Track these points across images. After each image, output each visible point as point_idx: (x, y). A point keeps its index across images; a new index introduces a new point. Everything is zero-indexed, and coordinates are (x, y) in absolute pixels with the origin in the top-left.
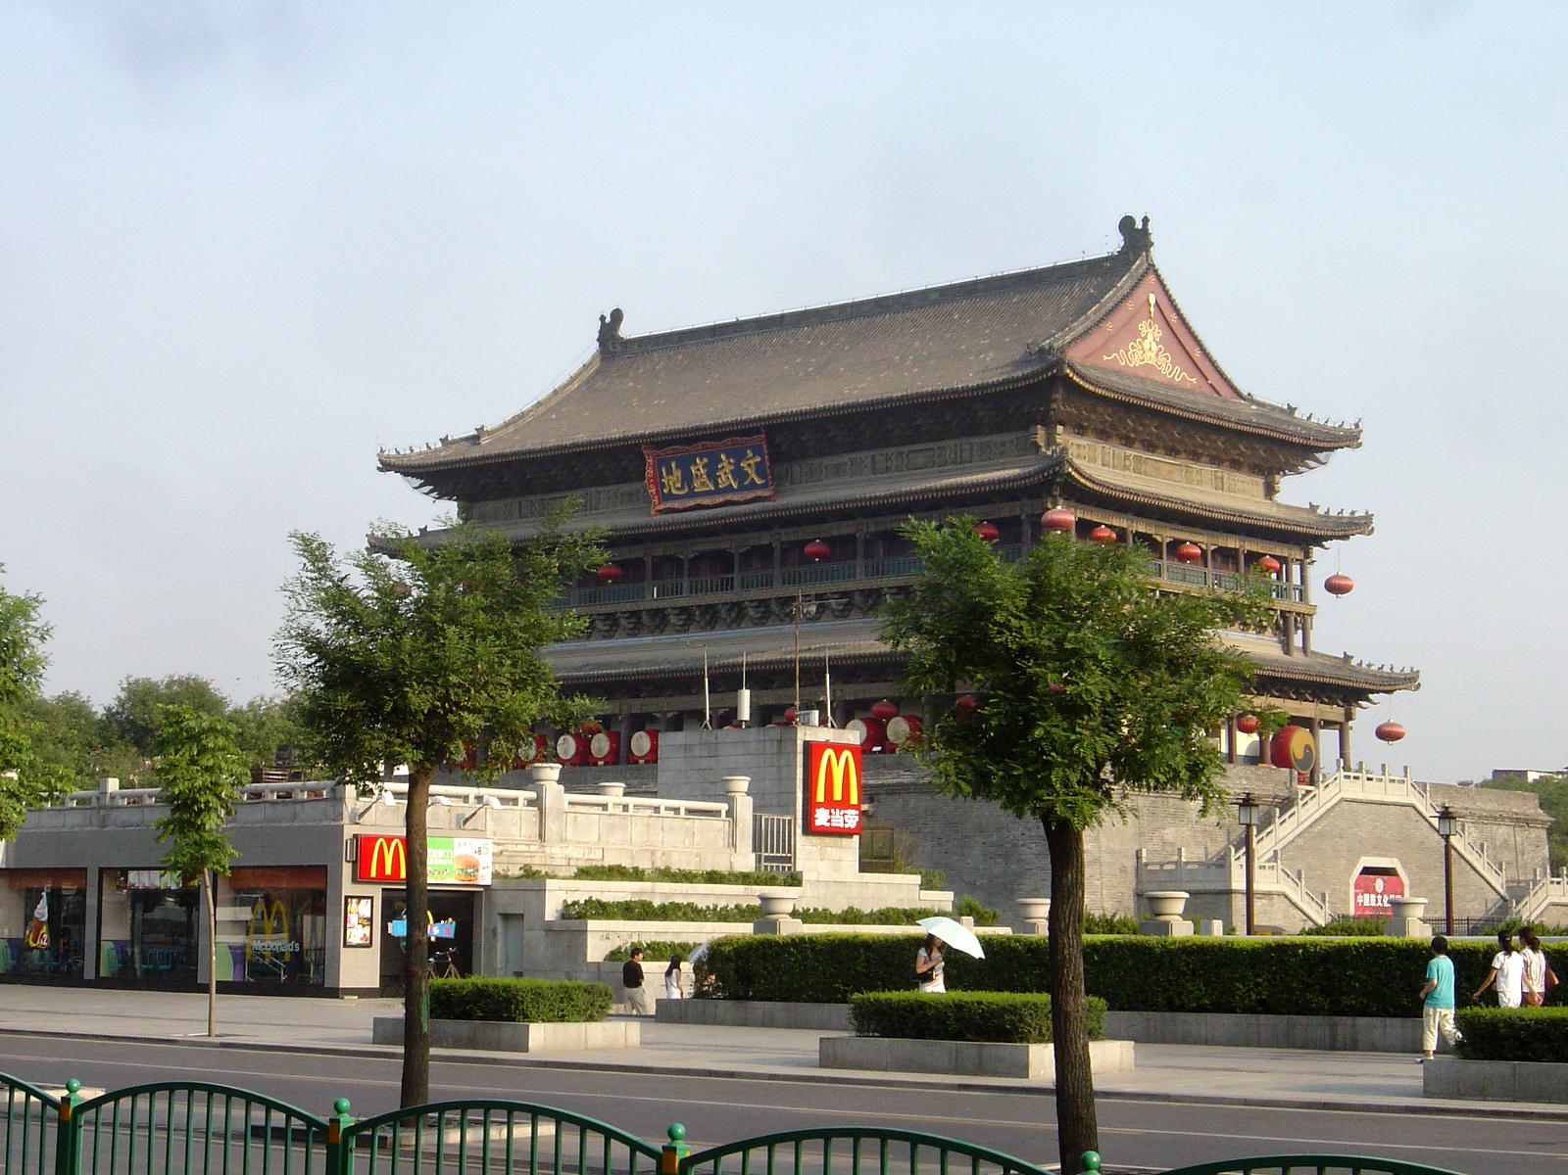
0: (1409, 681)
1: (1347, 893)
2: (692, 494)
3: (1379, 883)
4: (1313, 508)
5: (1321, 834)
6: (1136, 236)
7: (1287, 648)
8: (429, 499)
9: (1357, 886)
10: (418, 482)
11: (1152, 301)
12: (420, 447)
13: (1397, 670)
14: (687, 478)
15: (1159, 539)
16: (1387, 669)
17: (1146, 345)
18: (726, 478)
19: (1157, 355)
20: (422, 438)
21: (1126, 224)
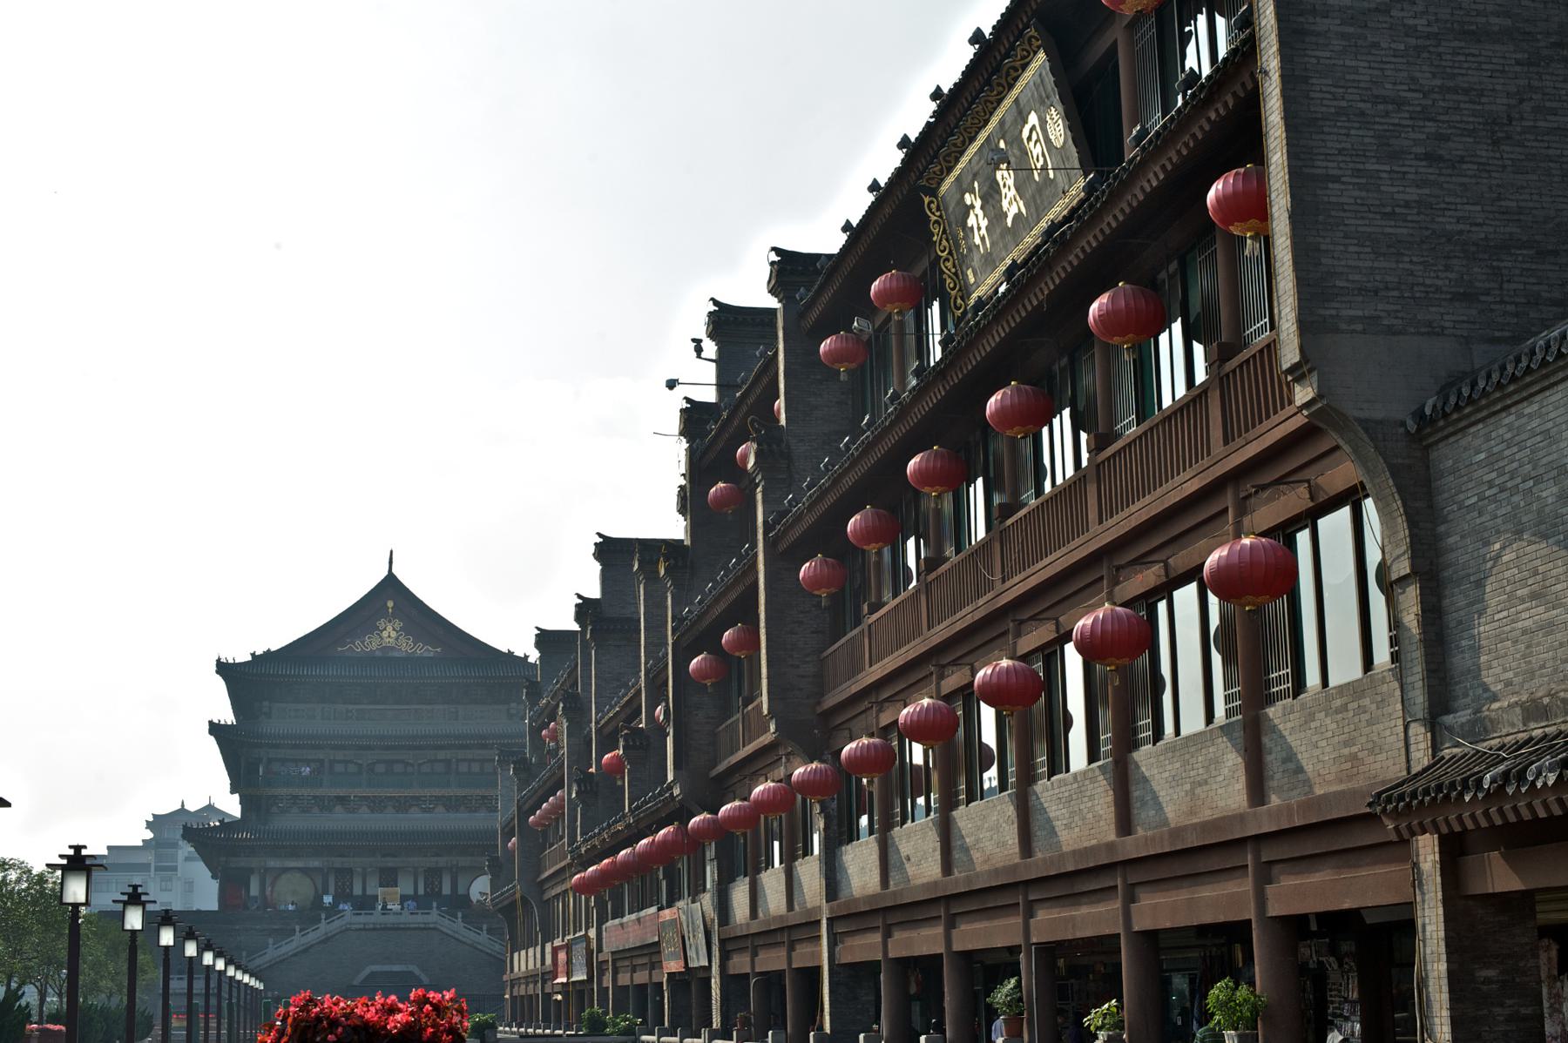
11: (390, 604)
17: (385, 634)
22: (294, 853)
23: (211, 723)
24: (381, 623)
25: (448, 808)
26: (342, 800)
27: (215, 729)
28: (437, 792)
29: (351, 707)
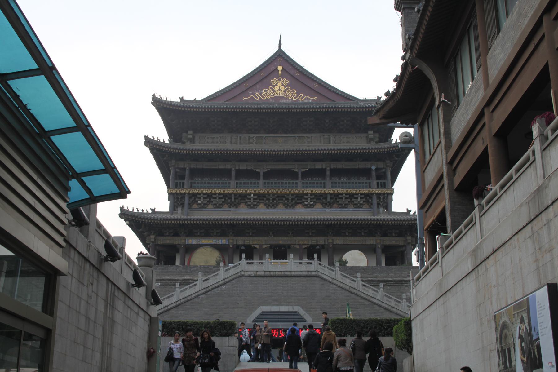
11: (280, 68)
17: (276, 88)
19: (285, 91)
22: (207, 234)
23: (146, 137)
24: (274, 81)
25: (325, 205)
26: (243, 197)
27: (151, 144)
28: (316, 191)
29: (252, 136)
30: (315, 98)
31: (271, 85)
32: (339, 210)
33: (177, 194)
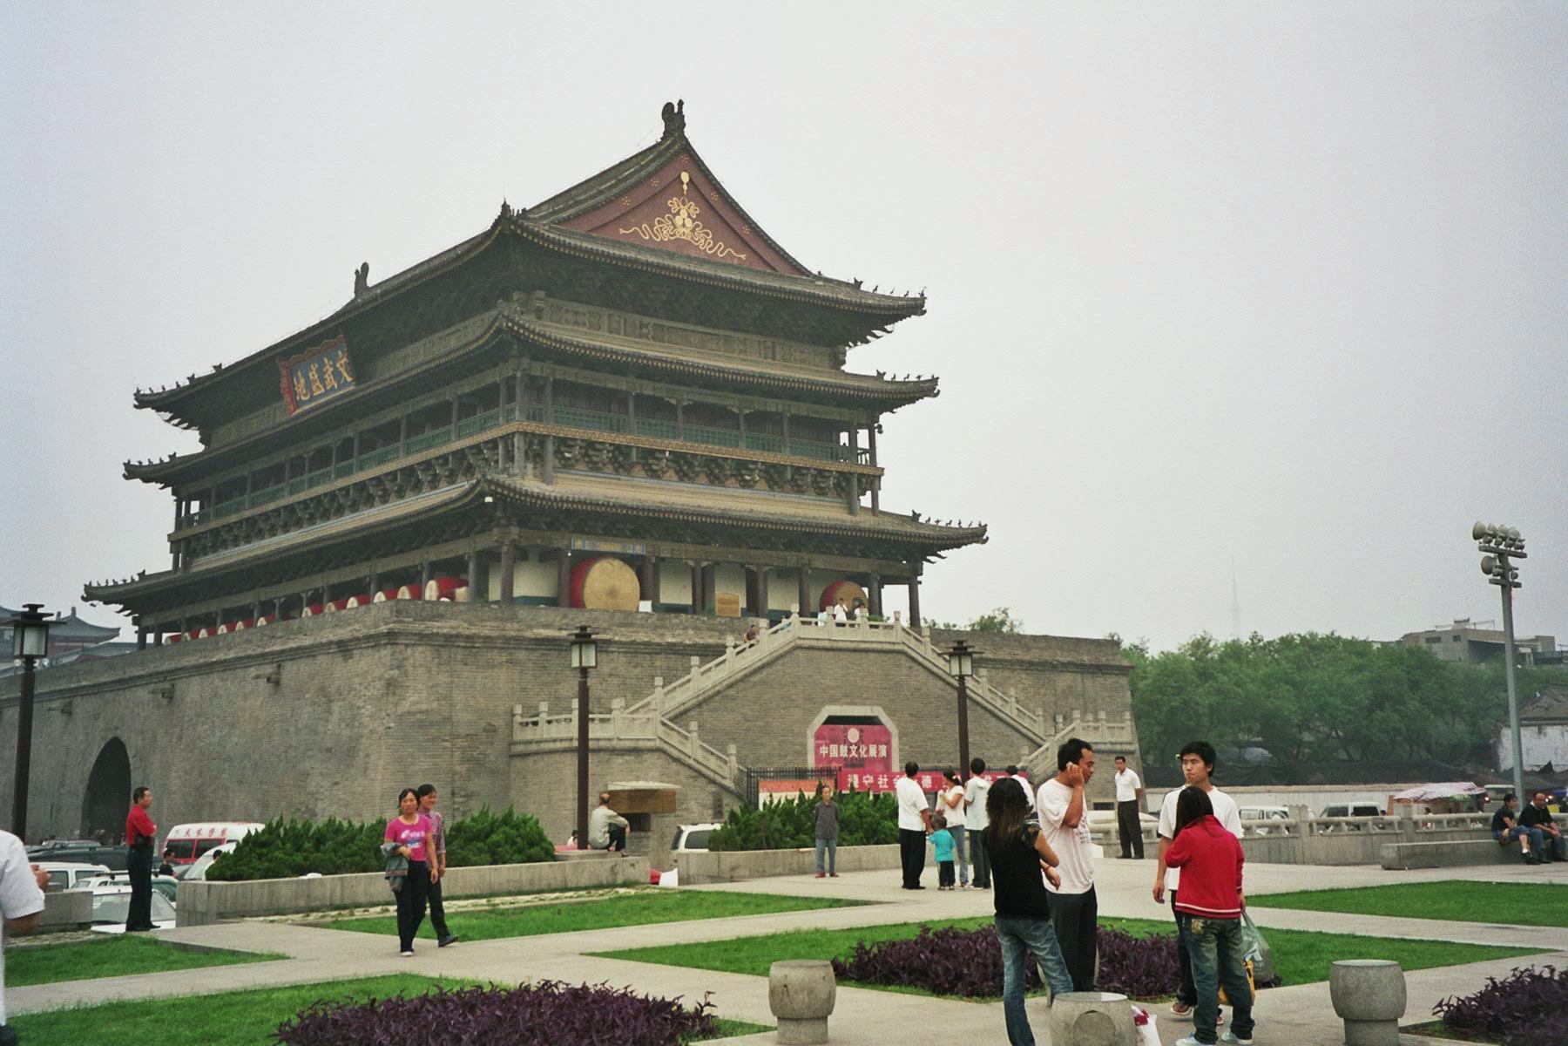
0: (977, 535)
1: (804, 745)
2: (313, 398)
3: (853, 734)
4: (881, 375)
5: (763, 682)
6: (673, 117)
7: (851, 508)
8: (178, 429)
9: (818, 736)
10: (168, 415)
11: (685, 177)
12: (171, 386)
13: (965, 525)
14: (308, 385)
15: (673, 402)
16: (955, 525)
17: (678, 220)
18: (331, 382)
19: (693, 231)
20: (172, 377)
21: (668, 108)
24: (674, 203)
29: (646, 320)
30: (743, 256)
31: (669, 210)
32: (793, 497)
33: (533, 434)
